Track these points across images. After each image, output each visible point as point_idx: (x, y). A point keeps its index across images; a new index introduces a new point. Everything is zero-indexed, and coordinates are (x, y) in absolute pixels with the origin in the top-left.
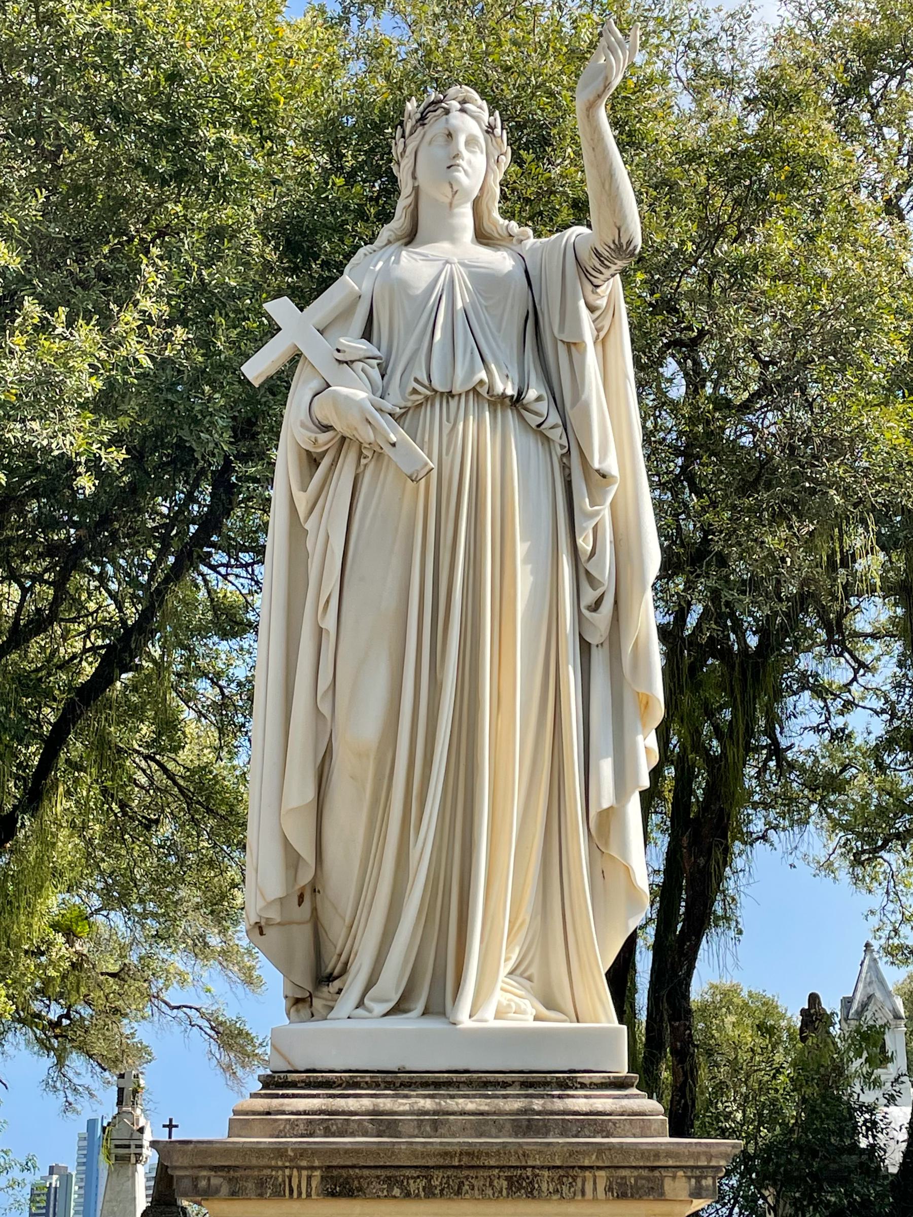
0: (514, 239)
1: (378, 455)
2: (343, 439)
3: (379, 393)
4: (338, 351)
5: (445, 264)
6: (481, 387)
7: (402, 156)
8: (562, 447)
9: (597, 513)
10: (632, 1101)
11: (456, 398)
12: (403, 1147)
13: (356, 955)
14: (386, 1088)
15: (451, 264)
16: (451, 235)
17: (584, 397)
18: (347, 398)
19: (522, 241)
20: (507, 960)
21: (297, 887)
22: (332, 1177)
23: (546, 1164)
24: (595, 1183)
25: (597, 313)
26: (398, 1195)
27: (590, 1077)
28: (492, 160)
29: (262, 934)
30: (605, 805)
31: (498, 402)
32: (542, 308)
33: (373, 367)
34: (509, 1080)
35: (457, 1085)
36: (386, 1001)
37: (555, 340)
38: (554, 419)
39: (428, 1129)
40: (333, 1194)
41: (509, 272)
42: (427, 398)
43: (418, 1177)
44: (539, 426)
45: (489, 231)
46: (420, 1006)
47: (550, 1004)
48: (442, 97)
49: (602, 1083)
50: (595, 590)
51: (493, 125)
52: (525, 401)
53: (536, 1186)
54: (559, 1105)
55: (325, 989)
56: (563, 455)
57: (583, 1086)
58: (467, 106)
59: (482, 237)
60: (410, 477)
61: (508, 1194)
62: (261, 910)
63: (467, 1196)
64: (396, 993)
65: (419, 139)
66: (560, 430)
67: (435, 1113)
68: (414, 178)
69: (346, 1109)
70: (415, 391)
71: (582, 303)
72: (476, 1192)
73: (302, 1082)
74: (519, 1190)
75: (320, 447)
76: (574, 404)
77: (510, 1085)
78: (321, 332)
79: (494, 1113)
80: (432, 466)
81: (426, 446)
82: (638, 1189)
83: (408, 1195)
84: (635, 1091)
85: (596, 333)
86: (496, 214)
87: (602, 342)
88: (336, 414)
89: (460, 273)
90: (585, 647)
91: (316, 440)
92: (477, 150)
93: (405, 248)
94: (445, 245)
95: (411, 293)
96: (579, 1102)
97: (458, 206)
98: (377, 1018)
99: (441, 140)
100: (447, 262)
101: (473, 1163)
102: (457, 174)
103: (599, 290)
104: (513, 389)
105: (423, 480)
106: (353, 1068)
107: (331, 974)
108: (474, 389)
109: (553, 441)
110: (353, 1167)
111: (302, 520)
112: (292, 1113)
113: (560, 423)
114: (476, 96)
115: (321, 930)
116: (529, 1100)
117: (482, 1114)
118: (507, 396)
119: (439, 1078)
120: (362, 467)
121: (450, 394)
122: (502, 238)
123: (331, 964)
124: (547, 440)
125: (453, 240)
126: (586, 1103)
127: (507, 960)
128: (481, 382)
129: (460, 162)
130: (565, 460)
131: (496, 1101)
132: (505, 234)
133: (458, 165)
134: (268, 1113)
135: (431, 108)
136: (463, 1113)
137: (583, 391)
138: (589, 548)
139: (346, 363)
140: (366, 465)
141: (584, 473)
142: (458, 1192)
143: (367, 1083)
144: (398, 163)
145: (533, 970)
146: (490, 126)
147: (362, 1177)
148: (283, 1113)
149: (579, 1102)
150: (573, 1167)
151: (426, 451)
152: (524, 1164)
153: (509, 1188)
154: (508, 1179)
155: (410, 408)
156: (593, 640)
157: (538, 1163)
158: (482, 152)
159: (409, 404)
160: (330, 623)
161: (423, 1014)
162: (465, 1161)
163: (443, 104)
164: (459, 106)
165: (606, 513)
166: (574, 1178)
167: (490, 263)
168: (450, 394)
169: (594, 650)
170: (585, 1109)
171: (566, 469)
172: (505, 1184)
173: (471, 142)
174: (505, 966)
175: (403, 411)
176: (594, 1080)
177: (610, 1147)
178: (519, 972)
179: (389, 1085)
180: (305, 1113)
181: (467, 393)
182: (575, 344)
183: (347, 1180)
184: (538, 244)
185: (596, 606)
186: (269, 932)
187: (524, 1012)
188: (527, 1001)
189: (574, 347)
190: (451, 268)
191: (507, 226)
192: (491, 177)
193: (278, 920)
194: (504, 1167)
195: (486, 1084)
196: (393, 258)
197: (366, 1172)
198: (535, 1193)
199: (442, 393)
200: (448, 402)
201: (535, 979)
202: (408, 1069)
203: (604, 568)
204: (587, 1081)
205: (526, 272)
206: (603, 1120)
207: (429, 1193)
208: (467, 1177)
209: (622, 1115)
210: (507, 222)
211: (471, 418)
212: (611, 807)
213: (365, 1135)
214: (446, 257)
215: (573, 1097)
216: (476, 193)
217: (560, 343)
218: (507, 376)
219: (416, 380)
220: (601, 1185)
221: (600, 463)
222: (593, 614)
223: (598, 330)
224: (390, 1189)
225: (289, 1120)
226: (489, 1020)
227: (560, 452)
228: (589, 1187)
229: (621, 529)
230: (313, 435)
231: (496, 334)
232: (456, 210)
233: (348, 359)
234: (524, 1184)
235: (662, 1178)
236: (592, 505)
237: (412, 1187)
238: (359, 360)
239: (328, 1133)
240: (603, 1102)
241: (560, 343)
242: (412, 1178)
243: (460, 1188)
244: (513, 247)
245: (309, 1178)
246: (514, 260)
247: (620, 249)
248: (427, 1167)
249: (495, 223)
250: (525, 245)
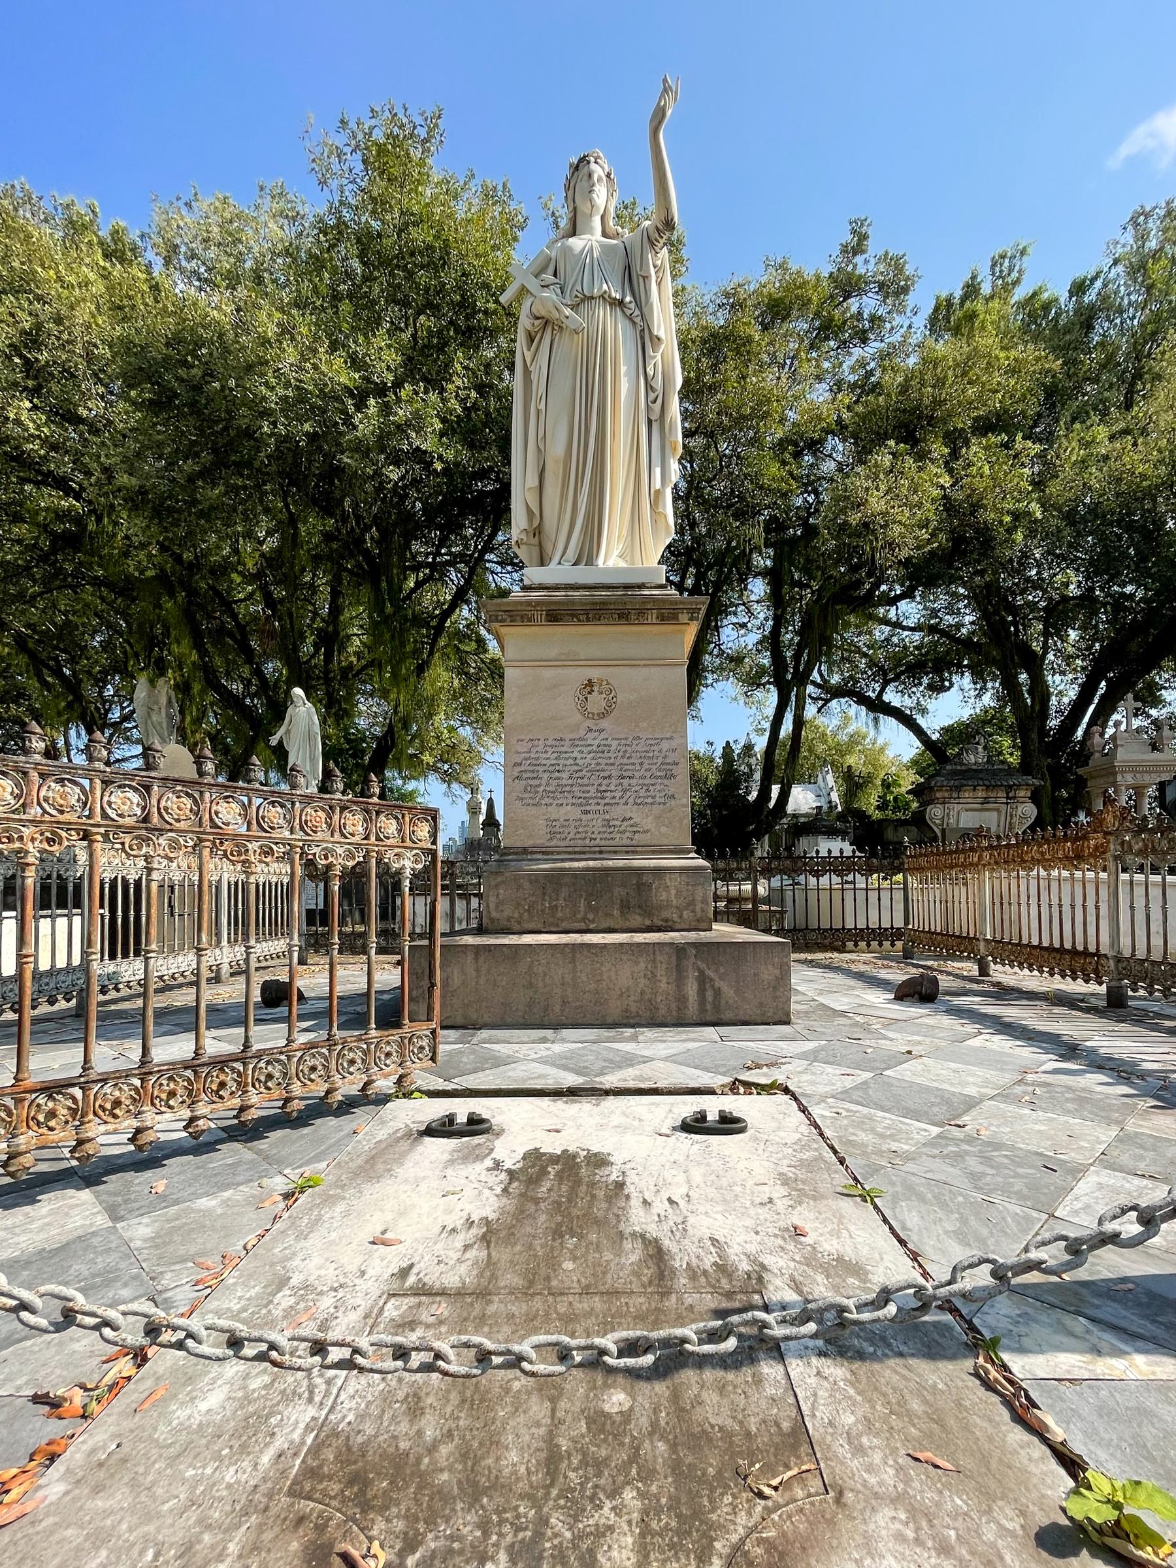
38: (637, 312)
87: (659, 284)
90: (650, 422)
124: (634, 323)
165: (659, 357)
171: (642, 338)
173: (600, 179)
185: (655, 401)
189: (646, 278)
203: (658, 384)
226: (611, 563)
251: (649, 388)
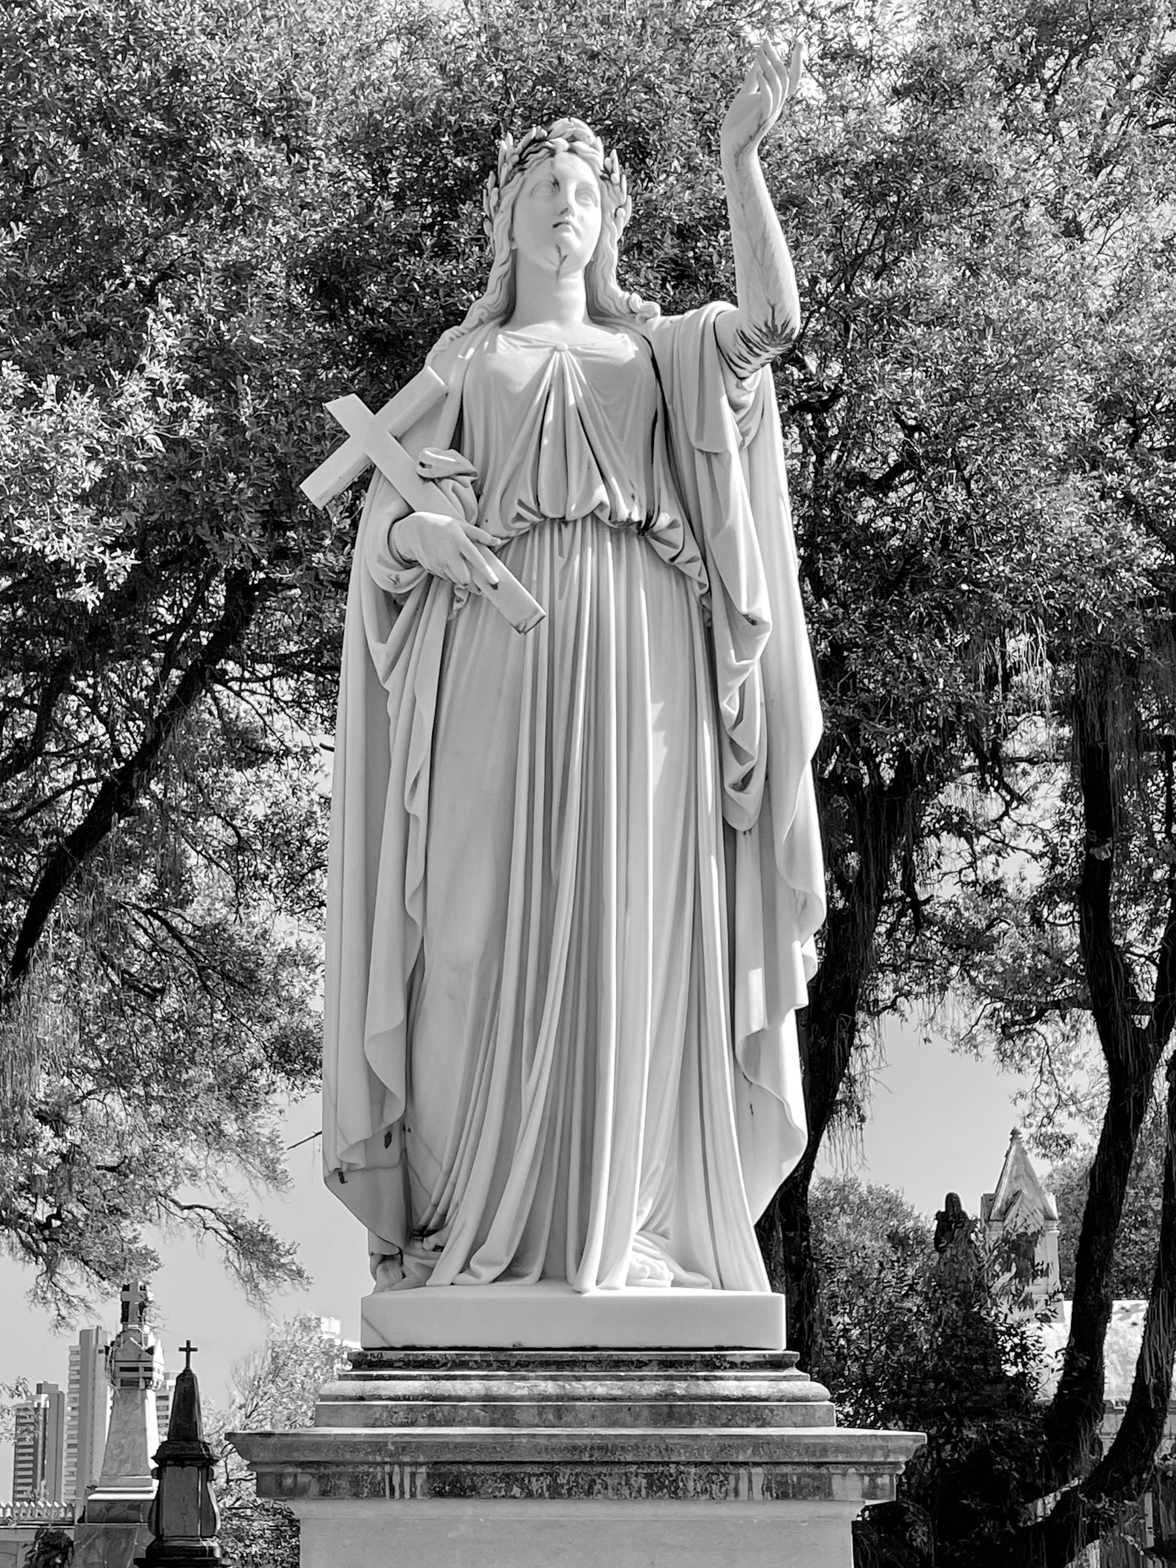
0: (637, 317)
1: (475, 598)
2: (431, 577)
3: (474, 520)
4: (423, 465)
5: (552, 352)
6: (601, 511)
7: (495, 211)
8: (701, 585)
9: (744, 669)
10: (791, 1383)
11: (571, 526)
12: (524, 1440)
13: (457, 1205)
14: (499, 1369)
15: (559, 351)
16: (557, 313)
17: (728, 523)
18: (435, 526)
19: (646, 319)
20: (639, 1213)
21: (384, 1126)
22: (440, 1475)
23: (692, 1459)
24: (750, 1481)
25: (743, 413)
26: (518, 1495)
27: (741, 1356)
28: (609, 214)
29: (342, 1181)
30: (755, 1028)
31: (622, 530)
32: (674, 408)
33: (465, 486)
34: (644, 1359)
35: (584, 1364)
36: (497, 1264)
37: (691, 449)
38: (692, 550)
39: (551, 1417)
40: (441, 1494)
41: (632, 362)
42: (534, 526)
43: (542, 1474)
44: (673, 559)
45: (605, 306)
46: (536, 1270)
47: (688, 1264)
48: (546, 133)
49: (755, 1363)
50: (742, 764)
51: (609, 169)
52: (655, 529)
53: (681, 1484)
54: (705, 1388)
55: (418, 1245)
56: (702, 596)
57: (733, 1366)
58: (577, 144)
59: (597, 314)
60: (517, 628)
61: (648, 1494)
62: (343, 1153)
63: (600, 1496)
64: (508, 1254)
66: (700, 563)
67: (559, 1398)
68: (512, 239)
69: (453, 1394)
70: (519, 517)
71: (724, 401)
72: (610, 1490)
73: (400, 1361)
74: (661, 1489)
75: (401, 587)
76: (716, 532)
77: (646, 1365)
78: (399, 440)
79: (629, 1399)
80: (543, 612)
81: (534, 587)
82: (802, 1488)
83: (530, 1495)
84: (795, 1371)
85: (741, 438)
86: (614, 284)
87: (748, 449)
89: (573, 365)
90: (730, 834)
91: (398, 579)
92: (591, 202)
93: (500, 330)
94: (551, 327)
95: (512, 390)
96: (730, 1385)
97: (567, 275)
98: (485, 1284)
100: (555, 349)
102: (566, 234)
103: (745, 384)
104: (640, 513)
105: (531, 634)
106: (460, 1344)
107: (425, 1227)
108: (592, 514)
109: (690, 578)
110: (465, 1463)
111: (380, 674)
113: (699, 556)
114: (588, 131)
115: (412, 1176)
116: (668, 1382)
117: (614, 1399)
118: (633, 523)
119: (561, 1356)
120: (455, 613)
121: (563, 521)
122: (622, 316)
123: (424, 1216)
125: (561, 319)
126: (738, 1387)
127: (639, 1213)
128: (601, 505)
129: (570, 218)
130: (704, 602)
131: (631, 1383)
132: (625, 310)
133: (567, 223)
135: (531, 149)
136: (592, 1398)
137: (727, 517)
138: (735, 713)
139: (433, 480)
140: (459, 610)
141: (728, 616)
142: (589, 1492)
143: (476, 1362)
144: (491, 221)
145: (669, 1225)
146: (606, 171)
147: (475, 1474)
149: (730, 1385)
150: (725, 1463)
151: (534, 592)
152: (666, 1459)
153: (650, 1486)
154: (646, 1476)
155: (512, 539)
156: (740, 826)
157: (683, 1458)
158: (596, 205)
159: (513, 534)
160: (418, 807)
161: (540, 1279)
162: (597, 1456)
163: (547, 143)
164: (567, 145)
165: (756, 668)
166: (726, 1476)
167: (609, 349)
168: (563, 521)
169: (740, 838)
170: (737, 1393)
171: (706, 613)
172: (644, 1481)
174: (638, 1221)
175: (505, 541)
176: (748, 1359)
177: (768, 1440)
178: (652, 1226)
179: (503, 1365)
180: (406, 1398)
181: (584, 519)
182: (716, 454)
183: (458, 1478)
184: (668, 324)
185: (743, 784)
186: (353, 1179)
187: (660, 1277)
188: (662, 1263)
189: (714, 457)
190: (561, 357)
191: (628, 301)
192: (608, 236)
193: (363, 1166)
194: (642, 1463)
195: (617, 1364)
196: (487, 343)
197: (480, 1469)
198: (680, 1493)
199: (553, 520)
200: (560, 530)
201: (671, 1234)
202: (525, 1346)
203: (753, 737)
204: (738, 1360)
205: (654, 360)
206: (758, 1407)
207: (555, 1492)
208: (599, 1475)
209: (780, 1401)
210: (627, 294)
211: (590, 549)
212: (762, 1030)
213: (477, 1423)
214: (555, 342)
215: (721, 1378)
216: (588, 258)
217: (698, 454)
218: (633, 497)
219: (521, 503)
220: (758, 1483)
221: (749, 605)
222: (740, 794)
223: (744, 434)
224: (509, 1488)
225: (387, 1406)
226: (620, 1288)
227: (700, 592)
228: (743, 1486)
229: (773, 688)
230: (394, 573)
231: (617, 441)
232: (564, 281)
233: (436, 476)
234: (667, 1483)
235: (830, 1475)
236: (739, 659)
237: (535, 1486)
238: (448, 478)
239: (432, 1422)
240: (758, 1385)
241: (698, 454)
242: (535, 1475)
243: (591, 1487)
244: (636, 328)
245: (413, 1475)
246: (638, 345)
247: (773, 333)
248: (553, 1463)
249: (613, 296)
250: (651, 325)
251: (726, 745)
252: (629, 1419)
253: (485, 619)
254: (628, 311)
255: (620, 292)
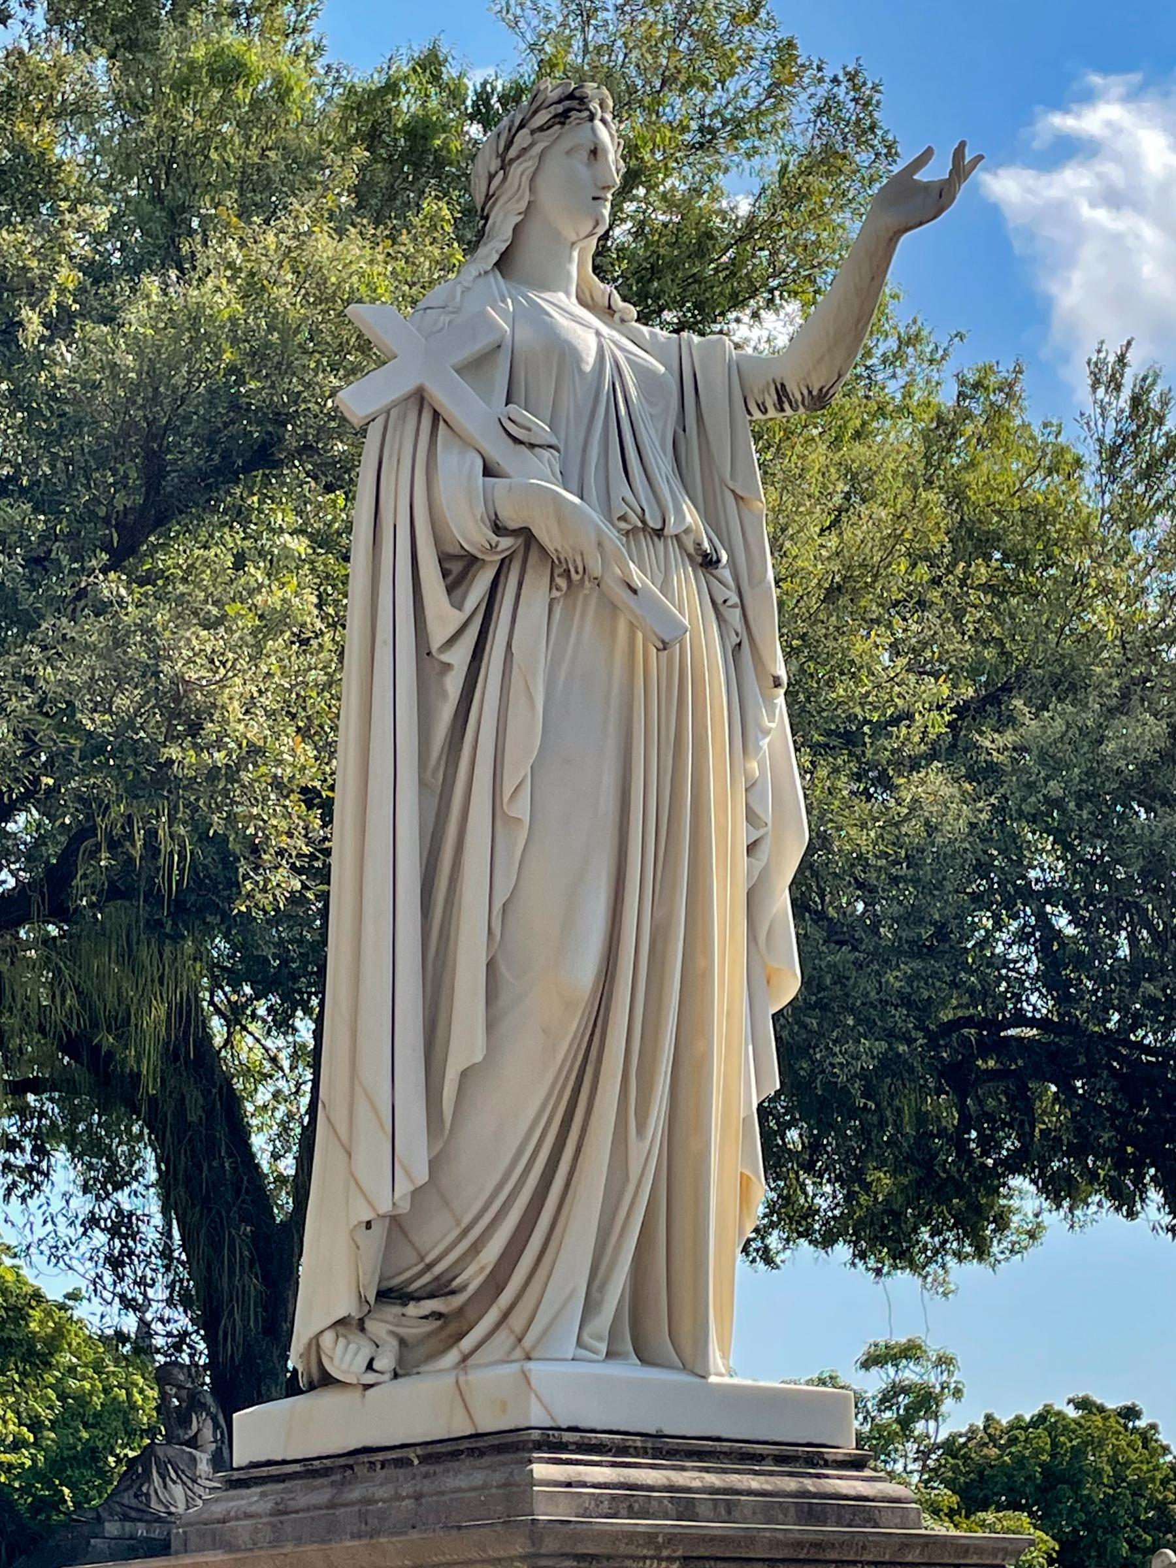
65: (552, 139)
70: (623, 518)
88: (559, 524)
99: (584, 155)
101: (821, 1557)
112: (594, 1486)
119: (703, 1445)
134: (569, 1485)
136: (750, 1493)
143: (636, 1448)
148: (584, 1485)
215: (827, 1476)
225: (593, 1494)
233: (533, 441)
252: (781, 1516)
253: (583, 616)
254: (607, 304)
255: (602, 285)
